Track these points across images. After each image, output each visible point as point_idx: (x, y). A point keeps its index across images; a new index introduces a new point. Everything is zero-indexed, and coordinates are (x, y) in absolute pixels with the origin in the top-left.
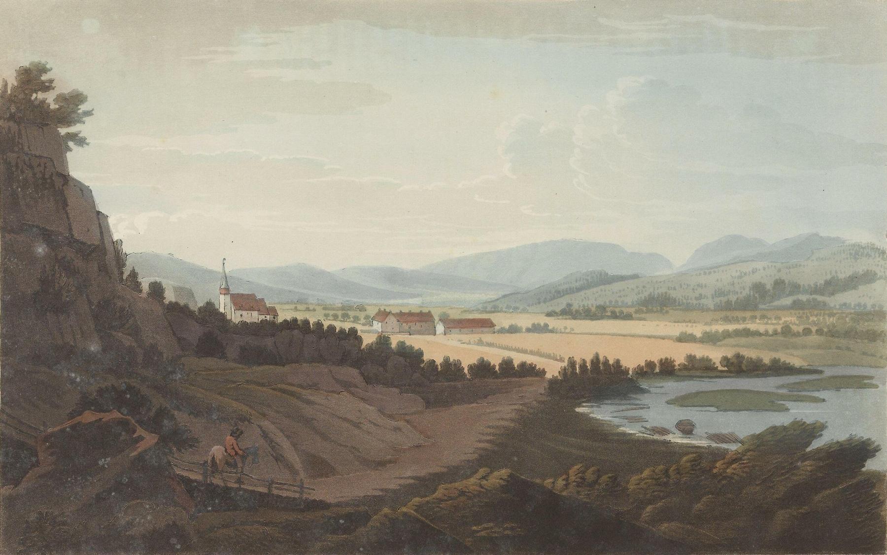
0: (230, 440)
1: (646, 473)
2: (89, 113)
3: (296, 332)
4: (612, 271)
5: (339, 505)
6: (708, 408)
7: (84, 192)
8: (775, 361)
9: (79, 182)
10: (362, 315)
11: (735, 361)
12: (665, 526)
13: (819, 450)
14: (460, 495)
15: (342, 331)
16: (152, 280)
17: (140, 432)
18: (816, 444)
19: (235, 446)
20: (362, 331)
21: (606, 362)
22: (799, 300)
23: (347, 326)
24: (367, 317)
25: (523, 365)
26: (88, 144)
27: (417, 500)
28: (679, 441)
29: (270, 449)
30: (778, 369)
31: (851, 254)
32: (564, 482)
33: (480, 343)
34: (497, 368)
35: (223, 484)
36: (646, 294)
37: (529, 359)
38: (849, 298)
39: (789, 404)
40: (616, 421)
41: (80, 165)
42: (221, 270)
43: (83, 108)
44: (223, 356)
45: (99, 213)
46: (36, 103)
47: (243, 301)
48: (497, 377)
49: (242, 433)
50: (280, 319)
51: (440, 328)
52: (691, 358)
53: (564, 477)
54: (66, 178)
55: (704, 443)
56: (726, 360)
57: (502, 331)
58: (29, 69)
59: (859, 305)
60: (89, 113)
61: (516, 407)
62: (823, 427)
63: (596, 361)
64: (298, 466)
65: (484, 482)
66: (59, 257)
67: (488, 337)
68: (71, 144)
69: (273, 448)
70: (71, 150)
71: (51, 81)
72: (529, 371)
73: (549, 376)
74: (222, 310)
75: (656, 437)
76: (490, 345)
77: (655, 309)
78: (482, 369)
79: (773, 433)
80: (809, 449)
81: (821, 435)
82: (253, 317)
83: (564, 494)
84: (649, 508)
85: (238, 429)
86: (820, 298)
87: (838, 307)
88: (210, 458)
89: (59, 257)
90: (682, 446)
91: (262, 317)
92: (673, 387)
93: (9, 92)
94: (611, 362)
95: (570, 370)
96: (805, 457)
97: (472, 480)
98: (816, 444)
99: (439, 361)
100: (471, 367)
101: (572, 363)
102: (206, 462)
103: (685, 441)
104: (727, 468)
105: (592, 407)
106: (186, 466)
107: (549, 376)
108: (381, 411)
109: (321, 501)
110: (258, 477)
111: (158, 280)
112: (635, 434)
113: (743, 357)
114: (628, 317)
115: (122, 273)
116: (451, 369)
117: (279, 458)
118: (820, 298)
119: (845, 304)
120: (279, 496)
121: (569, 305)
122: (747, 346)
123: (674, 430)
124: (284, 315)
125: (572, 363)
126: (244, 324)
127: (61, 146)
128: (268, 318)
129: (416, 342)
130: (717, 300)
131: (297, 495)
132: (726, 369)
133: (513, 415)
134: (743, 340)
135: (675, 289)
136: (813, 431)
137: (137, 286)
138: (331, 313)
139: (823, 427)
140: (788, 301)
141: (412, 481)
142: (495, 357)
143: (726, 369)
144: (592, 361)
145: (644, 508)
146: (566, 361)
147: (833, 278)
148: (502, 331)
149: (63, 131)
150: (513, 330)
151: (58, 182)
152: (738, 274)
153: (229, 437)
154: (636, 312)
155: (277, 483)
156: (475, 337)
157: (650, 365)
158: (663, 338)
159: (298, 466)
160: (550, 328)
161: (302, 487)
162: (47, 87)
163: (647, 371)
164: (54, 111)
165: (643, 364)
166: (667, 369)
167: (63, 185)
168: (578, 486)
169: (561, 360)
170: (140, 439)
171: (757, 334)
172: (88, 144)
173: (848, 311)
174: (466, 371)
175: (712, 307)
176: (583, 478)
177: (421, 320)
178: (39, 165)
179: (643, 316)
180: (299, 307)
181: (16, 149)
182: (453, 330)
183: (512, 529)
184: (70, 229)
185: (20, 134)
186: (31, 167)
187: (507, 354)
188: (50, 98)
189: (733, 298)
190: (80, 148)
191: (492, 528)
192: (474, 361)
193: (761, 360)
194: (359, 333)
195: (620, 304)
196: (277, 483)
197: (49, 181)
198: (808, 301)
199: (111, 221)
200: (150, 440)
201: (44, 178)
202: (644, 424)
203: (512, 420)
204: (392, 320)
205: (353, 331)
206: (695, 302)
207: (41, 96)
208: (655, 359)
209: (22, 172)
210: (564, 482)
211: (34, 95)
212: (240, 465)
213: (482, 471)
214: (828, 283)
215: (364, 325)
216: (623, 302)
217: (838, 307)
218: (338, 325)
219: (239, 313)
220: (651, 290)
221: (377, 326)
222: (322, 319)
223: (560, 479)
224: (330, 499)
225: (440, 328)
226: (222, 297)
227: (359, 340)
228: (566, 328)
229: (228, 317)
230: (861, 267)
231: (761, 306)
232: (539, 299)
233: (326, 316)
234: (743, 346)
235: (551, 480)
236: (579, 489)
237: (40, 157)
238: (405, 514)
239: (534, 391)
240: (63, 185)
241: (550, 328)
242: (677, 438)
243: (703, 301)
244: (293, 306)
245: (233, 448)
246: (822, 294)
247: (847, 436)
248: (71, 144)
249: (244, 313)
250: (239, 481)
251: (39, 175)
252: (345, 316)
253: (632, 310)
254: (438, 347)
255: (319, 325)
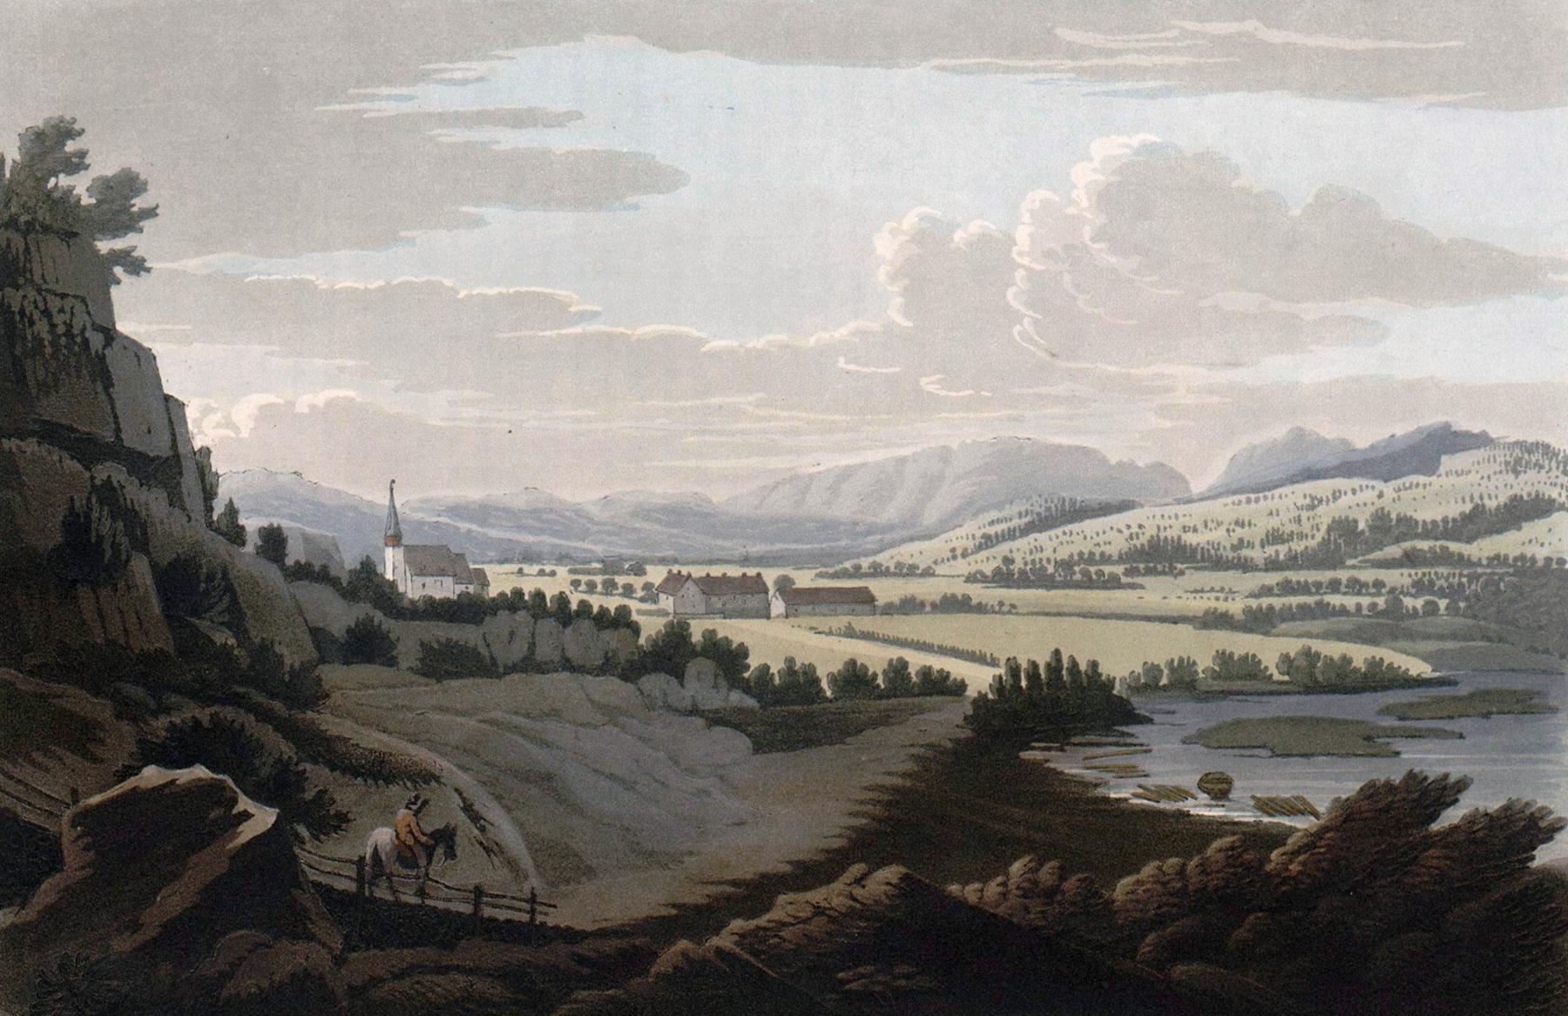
0: (403, 813)
1: (1148, 870)
2: (151, 213)
3: (522, 613)
4: (1082, 496)
5: (602, 934)
6: (1256, 752)
7: (142, 358)
8: (1374, 664)
9: (134, 342)
10: (638, 582)
11: (1302, 662)
12: (1179, 970)
13: (1454, 829)
14: (815, 914)
15: (603, 611)
16: (264, 523)
17: (244, 803)
18: (1452, 816)
19: (413, 825)
20: (639, 612)
21: (1074, 664)
22: (1414, 549)
23: (612, 603)
24: (647, 587)
25: (926, 672)
26: (148, 270)
27: (738, 924)
28: (1206, 812)
29: (476, 832)
30: (1378, 680)
31: (1507, 463)
32: (1000, 889)
33: (850, 633)
34: (880, 680)
35: (390, 898)
36: (1144, 540)
37: (937, 663)
38: (1508, 544)
39: (1398, 744)
40: (1090, 775)
41: (134, 313)
42: (387, 502)
43: (139, 203)
44: (392, 662)
45: (167, 398)
46: (56, 195)
47: (426, 559)
48: (880, 697)
49: (425, 802)
50: (493, 592)
51: (778, 606)
52: (1224, 658)
53: (1000, 879)
54: (109, 334)
55: (1248, 817)
56: (1286, 661)
57: (889, 610)
58: (43, 133)
59: (1522, 558)
60: (151, 213)
61: (914, 751)
62: (1462, 785)
63: (1055, 667)
64: (527, 862)
65: (858, 891)
66: (98, 482)
67: (865, 623)
68: (118, 271)
69: (483, 829)
70: (118, 282)
71: (82, 154)
72: (940, 686)
73: (971, 692)
74: (389, 576)
75: (1164, 805)
76: (867, 636)
77: (1160, 567)
78: (854, 678)
79: (1371, 796)
80: (1435, 827)
81: (1456, 801)
82: (445, 589)
83: (1001, 910)
84: (1150, 938)
85: (417, 798)
86: (1454, 547)
87: (1484, 562)
88: (369, 851)
89: (98, 482)
90: (1210, 822)
91: (460, 589)
92: (1193, 716)
93: (8, 175)
94: (1083, 667)
95: (1011, 681)
96: (1429, 841)
97: (838, 886)
98: (1452, 816)
99: (776, 667)
100: (833, 680)
101: (1014, 671)
102: (362, 859)
103: (1217, 813)
104: (1291, 861)
105: (1049, 749)
106: (327, 861)
107: (971, 692)
108: (674, 760)
109: (568, 928)
110: (454, 881)
111: (275, 522)
112: (1126, 800)
113: (1317, 655)
114: (1113, 583)
115: (210, 509)
116: (800, 683)
117: (491, 849)
118: (1454, 547)
119: (1497, 557)
120: (492, 920)
121: (1008, 561)
122: (1325, 636)
123: (1195, 791)
124: (500, 580)
125: (1014, 671)
126: (430, 601)
127: (102, 273)
128: (471, 589)
129: (734, 630)
130: (1270, 550)
131: (525, 917)
132: (1286, 678)
133: (910, 766)
134: (1317, 625)
135: (1195, 530)
136: (1446, 792)
137: (236, 535)
138: (584, 578)
139: (1462, 785)
140: (1394, 551)
141: (730, 889)
142: (875, 658)
143: (1286, 678)
144: (1048, 665)
145: (1144, 937)
146: (1003, 662)
147: (1476, 507)
148: (889, 610)
149: (104, 246)
150: (910, 606)
151: (96, 340)
152: (1308, 501)
153: (403, 811)
154: (1127, 573)
155: (492, 896)
156: (840, 622)
157: (1153, 670)
158: (1175, 620)
159: (527, 862)
160: (974, 602)
161: (533, 899)
162: (76, 164)
163: (1149, 683)
164: (88, 208)
165: (1139, 670)
166: (1184, 682)
167: (104, 347)
168: (1024, 896)
169: (993, 663)
170: (246, 816)
171: (1343, 611)
172: (148, 270)
173: (1504, 570)
174: (824, 684)
175: (1261, 563)
176: (1035, 883)
177: (744, 594)
178: (62, 311)
179: (1139, 580)
180: (527, 569)
181: (21, 281)
182: (802, 609)
183: (908, 977)
184: (118, 430)
185: (27, 251)
186: (46, 313)
187: (895, 653)
188: (80, 186)
189: (1298, 546)
190: (134, 278)
191: (871, 975)
192: (837, 667)
193: (1350, 661)
194: (635, 617)
195: (1097, 557)
196: (492, 896)
197: (78, 340)
198: (1432, 549)
199: (191, 413)
200: (263, 818)
201: (69, 334)
202: (1142, 781)
203: (905, 775)
204: (691, 589)
205: (623, 611)
206: (1231, 555)
207: (64, 180)
208: (1160, 659)
209: (32, 323)
210: (1000, 889)
211: (53, 181)
212: (423, 862)
213: (856, 869)
214: (1467, 518)
215: (642, 600)
216: (1102, 554)
217: (1484, 562)
218: (596, 602)
219: (419, 580)
220: (1154, 532)
221: (667, 602)
222: (567, 589)
223: (993, 884)
224: (583, 924)
225: (778, 606)
226: (389, 553)
227: (635, 629)
228: (1001, 604)
229: (401, 589)
230: (1527, 484)
231: (1350, 562)
232: (953, 550)
233: (576, 583)
234: (1317, 636)
235: (977, 886)
236: (1027, 902)
237: (64, 296)
238: (719, 951)
239: (944, 723)
240: (104, 347)
241: (974, 602)
242: (1202, 808)
243: (1245, 552)
244: (515, 567)
245: (411, 832)
246: (1458, 540)
247: (1502, 803)
248: (118, 271)
249: (429, 580)
250: (421, 893)
251: (61, 329)
252: (610, 586)
253: (1119, 570)
254: (773, 642)
255: (562, 600)
